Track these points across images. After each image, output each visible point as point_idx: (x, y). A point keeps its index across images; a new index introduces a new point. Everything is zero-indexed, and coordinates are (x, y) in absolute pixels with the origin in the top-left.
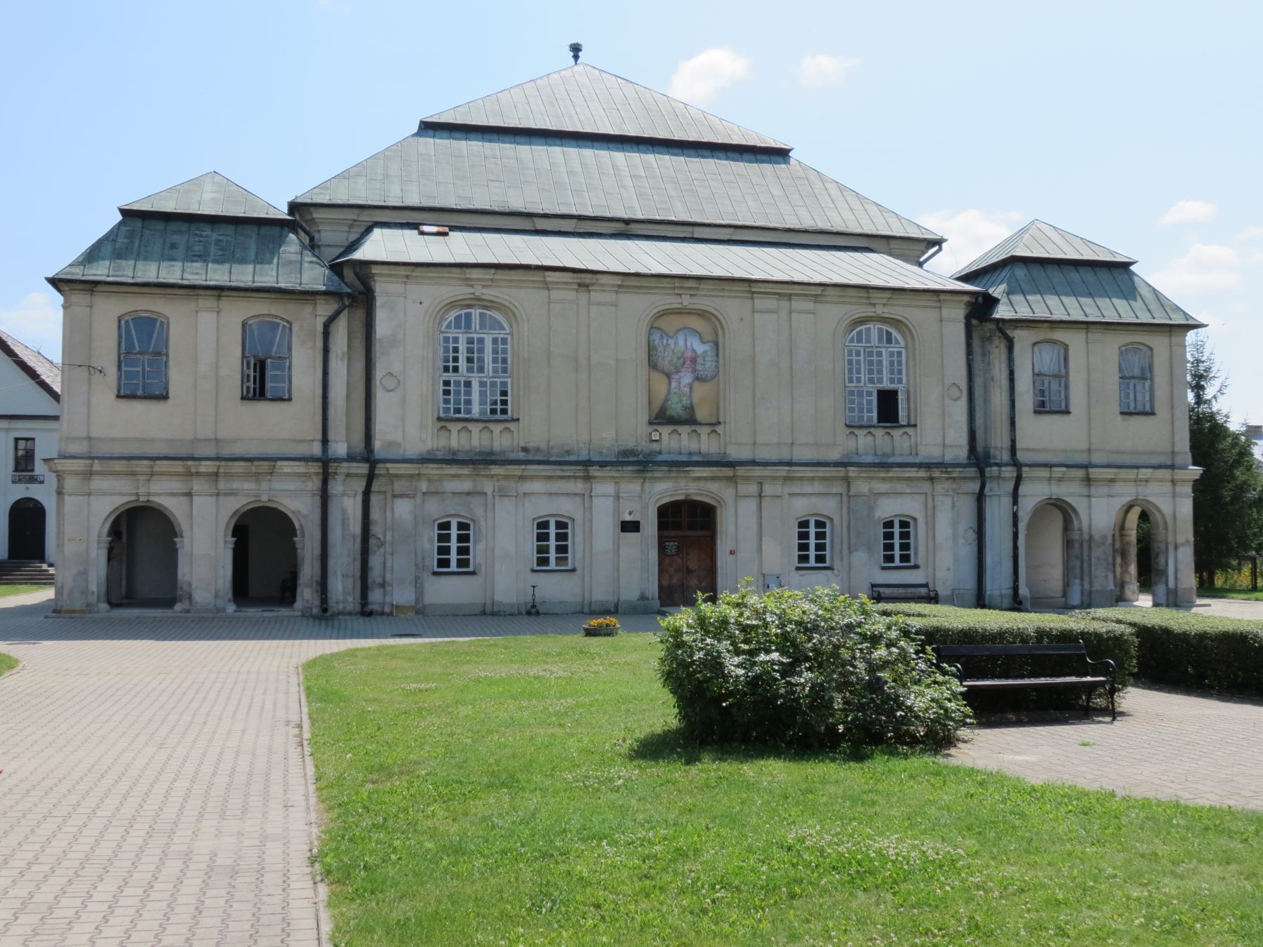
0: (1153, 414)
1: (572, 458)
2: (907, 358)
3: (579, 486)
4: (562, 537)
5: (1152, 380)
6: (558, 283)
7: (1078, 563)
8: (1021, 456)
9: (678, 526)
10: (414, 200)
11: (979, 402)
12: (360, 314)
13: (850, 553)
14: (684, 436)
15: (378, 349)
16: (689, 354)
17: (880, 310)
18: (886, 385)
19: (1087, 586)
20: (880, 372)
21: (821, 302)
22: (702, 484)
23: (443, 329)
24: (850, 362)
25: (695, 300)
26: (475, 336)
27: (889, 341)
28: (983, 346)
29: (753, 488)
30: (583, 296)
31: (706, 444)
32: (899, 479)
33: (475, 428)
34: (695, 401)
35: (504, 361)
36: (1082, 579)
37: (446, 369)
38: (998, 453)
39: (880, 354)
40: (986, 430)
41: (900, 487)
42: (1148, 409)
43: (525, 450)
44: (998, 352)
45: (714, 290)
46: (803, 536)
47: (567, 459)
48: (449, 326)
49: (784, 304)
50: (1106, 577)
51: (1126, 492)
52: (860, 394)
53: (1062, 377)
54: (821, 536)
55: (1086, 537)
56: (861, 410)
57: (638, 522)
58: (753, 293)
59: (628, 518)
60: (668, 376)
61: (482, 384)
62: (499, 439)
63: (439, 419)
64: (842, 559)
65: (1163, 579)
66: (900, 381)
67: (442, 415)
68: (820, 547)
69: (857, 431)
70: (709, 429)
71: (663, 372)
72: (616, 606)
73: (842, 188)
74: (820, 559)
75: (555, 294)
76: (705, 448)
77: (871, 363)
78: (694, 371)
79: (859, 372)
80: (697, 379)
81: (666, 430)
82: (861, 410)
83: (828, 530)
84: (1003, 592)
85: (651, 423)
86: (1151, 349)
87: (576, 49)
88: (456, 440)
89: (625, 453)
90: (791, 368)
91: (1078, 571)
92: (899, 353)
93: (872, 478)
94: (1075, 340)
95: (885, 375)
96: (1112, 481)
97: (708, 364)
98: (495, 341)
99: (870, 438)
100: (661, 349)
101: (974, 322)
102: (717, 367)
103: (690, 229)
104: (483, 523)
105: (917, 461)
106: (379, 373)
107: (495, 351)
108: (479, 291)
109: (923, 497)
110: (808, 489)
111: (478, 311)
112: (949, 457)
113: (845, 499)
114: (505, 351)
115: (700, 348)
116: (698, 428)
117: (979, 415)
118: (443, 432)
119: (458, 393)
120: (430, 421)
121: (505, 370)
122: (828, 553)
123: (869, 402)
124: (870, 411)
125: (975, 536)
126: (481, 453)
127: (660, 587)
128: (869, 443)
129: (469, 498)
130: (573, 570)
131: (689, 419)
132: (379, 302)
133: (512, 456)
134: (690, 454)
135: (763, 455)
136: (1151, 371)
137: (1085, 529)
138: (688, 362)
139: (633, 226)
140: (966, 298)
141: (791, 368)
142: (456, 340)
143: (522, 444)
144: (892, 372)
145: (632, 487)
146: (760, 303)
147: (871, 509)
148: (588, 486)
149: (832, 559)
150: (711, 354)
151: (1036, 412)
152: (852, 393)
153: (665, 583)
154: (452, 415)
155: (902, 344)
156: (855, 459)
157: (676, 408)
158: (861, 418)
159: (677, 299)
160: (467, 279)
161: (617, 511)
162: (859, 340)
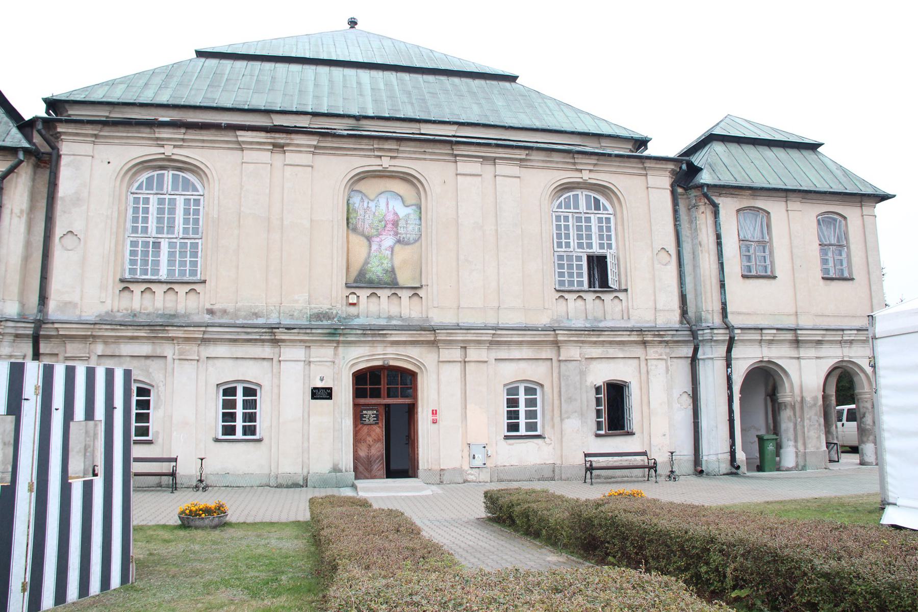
0: (852, 279)
1: (261, 321)
2: (616, 224)
3: (267, 351)
4: (250, 404)
5: (848, 248)
6: (251, 143)
7: (791, 425)
8: (733, 320)
9: (376, 394)
10: (163, 99)
11: (688, 268)
12: (45, 175)
13: (562, 420)
14: (384, 299)
15: (59, 207)
16: (390, 217)
17: (586, 176)
18: (596, 250)
19: (801, 448)
20: (589, 237)
21: (526, 167)
22: (401, 350)
23: (134, 190)
24: (558, 227)
25: (394, 162)
26: (167, 197)
27: (597, 207)
28: (689, 215)
29: (456, 354)
30: (278, 158)
31: (407, 309)
32: (611, 343)
33: (159, 289)
34: (397, 262)
35: (196, 221)
36: (796, 441)
37: (135, 230)
38: (709, 317)
39: (588, 220)
40: (697, 295)
41: (612, 351)
42: (846, 275)
43: (211, 312)
44: (704, 218)
45: (415, 152)
46: (512, 403)
47: (255, 321)
48: (140, 187)
49: (488, 169)
50: (819, 437)
51: (832, 355)
52: (570, 258)
53: (765, 244)
54: (531, 403)
55: (799, 399)
56: (571, 275)
57: (331, 389)
58: (456, 156)
59: (320, 385)
60: (369, 239)
61: (172, 245)
62: (183, 303)
63: (122, 281)
64: (553, 427)
65: (871, 438)
66: (610, 246)
67: (127, 276)
68: (531, 415)
69: (566, 295)
70: (411, 293)
71: (363, 235)
72: (306, 480)
73: (559, 104)
74: (531, 427)
75: (249, 155)
76: (405, 313)
77: (579, 228)
78: (396, 234)
79: (567, 236)
80: (399, 241)
81: (364, 294)
82: (571, 275)
83: (539, 396)
84: (720, 456)
85: (348, 286)
86: (845, 218)
87: (353, 23)
88: (138, 302)
89: (319, 316)
90: (497, 231)
91: (791, 434)
92: (608, 220)
93: (583, 342)
94: (776, 208)
95: (595, 241)
96: (819, 342)
97: (410, 228)
98: (187, 201)
99: (580, 302)
100: (361, 212)
101: (680, 190)
102: (420, 230)
103: (417, 125)
104: (162, 388)
105: (629, 325)
106: (59, 230)
107: (187, 212)
108: (169, 151)
109: (636, 361)
110: (516, 353)
111: (171, 172)
112: (661, 322)
113: (555, 364)
114: (197, 212)
115: (402, 211)
116: (399, 292)
117: (688, 280)
118: (126, 294)
119: (145, 253)
120: (111, 281)
121: (196, 231)
122: (539, 420)
123: (579, 267)
124: (580, 275)
125: (690, 401)
126: (163, 315)
127: (356, 458)
128: (581, 310)
129: (149, 362)
130: (260, 440)
131: (392, 284)
132: (64, 161)
133: (196, 319)
134: (390, 318)
135: (468, 319)
136: (847, 239)
137: (797, 391)
138: (390, 226)
139: (363, 122)
140: (671, 166)
141: (497, 231)
142: (147, 201)
143: (208, 306)
144: (601, 237)
145: (325, 353)
146: (464, 167)
147: (582, 374)
148: (277, 350)
149: (543, 427)
150: (414, 217)
151: (744, 277)
152: (560, 258)
153: (362, 453)
154: (137, 277)
155: (611, 211)
156: (566, 324)
157: (376, 270)
158: (571, 283)
159: (377, 161)
160: (158, 139)
161: (307, 377)
162: (568, 206)
